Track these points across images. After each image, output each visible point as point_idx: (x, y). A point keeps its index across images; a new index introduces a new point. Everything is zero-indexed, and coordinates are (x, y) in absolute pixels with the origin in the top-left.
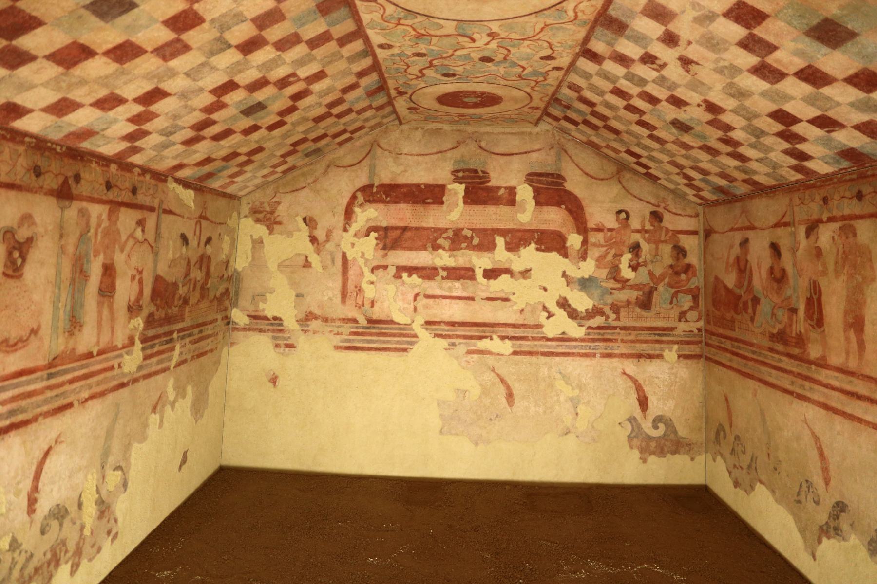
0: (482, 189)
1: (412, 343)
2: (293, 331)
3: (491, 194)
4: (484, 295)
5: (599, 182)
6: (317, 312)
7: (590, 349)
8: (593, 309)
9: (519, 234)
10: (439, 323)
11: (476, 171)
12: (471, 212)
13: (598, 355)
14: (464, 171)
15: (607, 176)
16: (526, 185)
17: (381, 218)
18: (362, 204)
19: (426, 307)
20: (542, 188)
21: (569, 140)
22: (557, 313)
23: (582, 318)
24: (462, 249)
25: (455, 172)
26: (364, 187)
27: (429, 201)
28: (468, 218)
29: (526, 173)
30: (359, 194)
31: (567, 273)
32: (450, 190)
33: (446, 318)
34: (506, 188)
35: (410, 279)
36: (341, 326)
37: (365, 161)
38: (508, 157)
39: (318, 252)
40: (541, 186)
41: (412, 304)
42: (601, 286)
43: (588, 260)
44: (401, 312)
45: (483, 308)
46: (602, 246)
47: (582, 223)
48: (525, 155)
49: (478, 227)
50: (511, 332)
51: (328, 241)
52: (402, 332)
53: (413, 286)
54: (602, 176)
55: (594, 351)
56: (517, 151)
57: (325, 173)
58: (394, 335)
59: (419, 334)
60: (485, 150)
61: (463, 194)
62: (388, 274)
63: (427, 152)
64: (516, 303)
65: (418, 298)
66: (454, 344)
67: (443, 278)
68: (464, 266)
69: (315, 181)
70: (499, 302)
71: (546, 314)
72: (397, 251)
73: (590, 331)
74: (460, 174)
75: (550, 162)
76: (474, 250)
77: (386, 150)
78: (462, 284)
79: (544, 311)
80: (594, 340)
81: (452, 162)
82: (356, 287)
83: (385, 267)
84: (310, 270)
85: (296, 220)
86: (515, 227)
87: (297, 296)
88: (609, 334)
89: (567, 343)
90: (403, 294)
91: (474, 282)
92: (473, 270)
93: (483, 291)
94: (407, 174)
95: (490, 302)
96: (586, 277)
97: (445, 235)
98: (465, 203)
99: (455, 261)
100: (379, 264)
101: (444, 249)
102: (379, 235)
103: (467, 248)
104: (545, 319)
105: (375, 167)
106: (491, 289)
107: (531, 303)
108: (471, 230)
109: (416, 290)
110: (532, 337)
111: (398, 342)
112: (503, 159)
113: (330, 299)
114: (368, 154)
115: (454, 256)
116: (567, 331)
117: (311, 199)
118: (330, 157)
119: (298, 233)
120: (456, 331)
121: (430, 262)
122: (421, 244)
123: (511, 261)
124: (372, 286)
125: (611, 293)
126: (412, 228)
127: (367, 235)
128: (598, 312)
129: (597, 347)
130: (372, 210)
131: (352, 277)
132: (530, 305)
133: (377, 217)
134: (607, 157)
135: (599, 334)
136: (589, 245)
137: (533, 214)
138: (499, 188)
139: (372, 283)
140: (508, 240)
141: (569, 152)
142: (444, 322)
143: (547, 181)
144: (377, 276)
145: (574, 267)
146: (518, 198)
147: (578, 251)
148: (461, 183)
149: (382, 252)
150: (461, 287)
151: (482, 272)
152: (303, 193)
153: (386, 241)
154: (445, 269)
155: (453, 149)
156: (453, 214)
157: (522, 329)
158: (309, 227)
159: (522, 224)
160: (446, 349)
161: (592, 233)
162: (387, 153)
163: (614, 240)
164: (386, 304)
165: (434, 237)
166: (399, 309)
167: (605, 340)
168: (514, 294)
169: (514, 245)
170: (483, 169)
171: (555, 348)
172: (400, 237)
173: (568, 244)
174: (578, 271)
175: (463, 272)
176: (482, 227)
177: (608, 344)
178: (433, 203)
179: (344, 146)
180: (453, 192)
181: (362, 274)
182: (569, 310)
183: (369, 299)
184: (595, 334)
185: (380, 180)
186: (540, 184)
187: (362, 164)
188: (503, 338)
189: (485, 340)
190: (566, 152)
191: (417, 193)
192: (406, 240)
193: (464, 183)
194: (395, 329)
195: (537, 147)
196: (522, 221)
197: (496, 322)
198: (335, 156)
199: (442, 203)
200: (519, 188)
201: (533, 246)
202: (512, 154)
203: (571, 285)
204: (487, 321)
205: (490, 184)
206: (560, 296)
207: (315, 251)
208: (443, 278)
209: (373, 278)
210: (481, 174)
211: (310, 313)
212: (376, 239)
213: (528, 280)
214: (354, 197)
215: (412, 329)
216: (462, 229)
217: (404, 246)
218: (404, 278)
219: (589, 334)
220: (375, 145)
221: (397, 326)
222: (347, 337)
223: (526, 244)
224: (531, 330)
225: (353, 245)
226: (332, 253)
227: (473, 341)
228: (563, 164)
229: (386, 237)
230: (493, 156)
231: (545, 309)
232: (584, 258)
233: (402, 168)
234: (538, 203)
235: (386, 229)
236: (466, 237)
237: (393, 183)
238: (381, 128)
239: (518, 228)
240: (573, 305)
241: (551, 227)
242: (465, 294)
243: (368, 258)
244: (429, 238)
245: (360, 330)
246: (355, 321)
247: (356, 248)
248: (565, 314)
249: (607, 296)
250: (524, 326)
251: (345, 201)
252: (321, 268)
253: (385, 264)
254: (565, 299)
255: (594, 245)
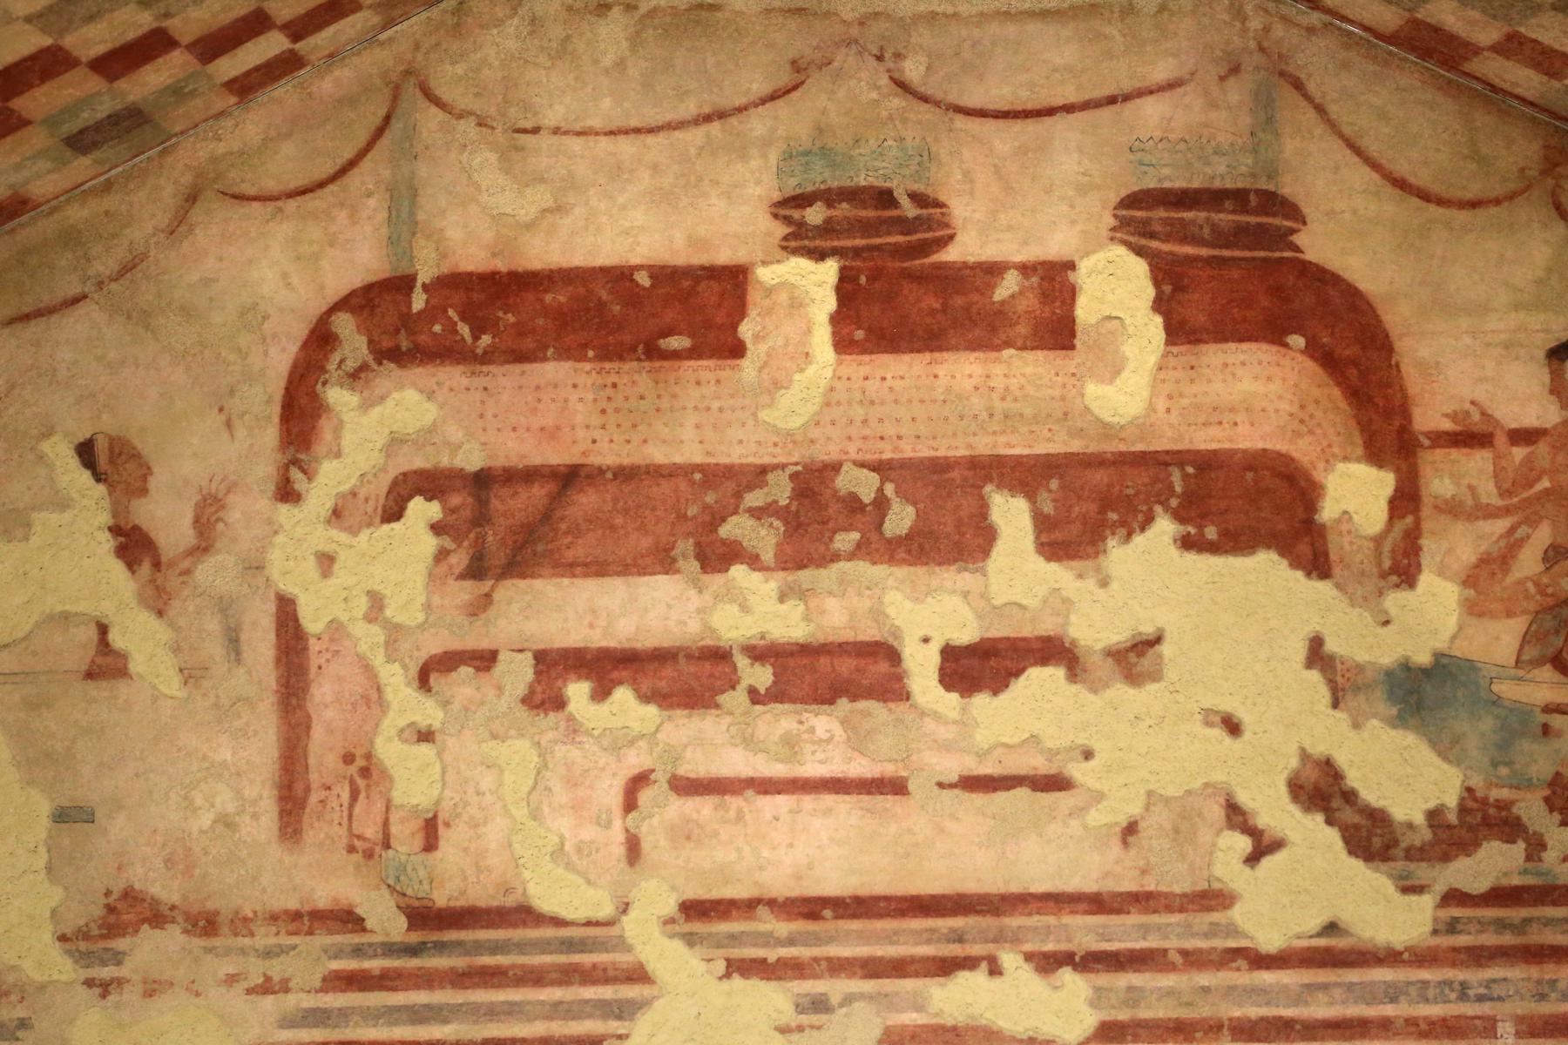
0: (919, 278)
1: (624, 1011)
2: (42, 987)
3: (959, 301)
4: (953, 766)
5: (1463, 216)
6: (165, 889)
7: (1463, 996)
8: (1463, 810)
9: (1100, 477)
10: (749, 906)
11: (885, 198)
12: (873, 386)
13: (1506, 1029)
14: (829, 197)
15: (1498, 190)
16: (1120, 251)
17: (454, 433)
18: (364, 367)
19: (685, 834)
20: (1196, 259)
21: (1311, 30)
22: (1292, 835)
23: (1417, 854)
24: (836, 557)
25: (789, 205)
26: (369, 288)
27: (676, 342)
28: (859, 412)
29: (1114, 198)
30: (345, 325)
31: (1331, 646)
32: (770, 291)
33: (779, 884)
34: (1026, 269)
35: (603, 709)
36: (282, 951)
37: (367, 164)
38: (1031, 127)
39: (158, 602)
40: (1189, 250)
41: (618, 824)
42: (1496, 701)
43: (1426, 579)
44: (569, 866)
45: (950, 825)
46: (1490, 513)
47: (1388, 414)
48: (1106, 113)
49: (908, 453)
50: (1085, 932)
51: (203, 546)
52: (576, 958)
53: (620, 742)
54: (1474, 190)
55: (1486, 1009)
56: (1070, 95)
57: (179, 225)
58: (536, 978)
59: (653, 966)
60: (925, 99)
61: (831, 304)
62: (500, 689)
63: (654, 116)
64: (1099, 797)
65: (645, 796)
66: (819, 1005)
67: (755, 696)
68: (849, 636)
69: (126, 269)
70: (1022, 793)
71: (1244, 844)
72: (538, 584)
73: (1457, 912)
74: (815, 215)
75: (1223, 139)
76: (892, 560)
77: (460, 116)
78: (844, 722)
79: (1231, 825)
80: (1478, 956)
81: (773, 157)
82: (348, 759)
83: (485, 660)
84: (123, 689)
85: (41, 458)
86: (1076, 446)
87: (62, 816)
88: (1549, 922)
89: (1353, 976)
90: (572, 783)
91: (899, 708)
92: (892, 655)
93: (946, 747)
94: (566, 222)
95: (979, 799)
96: (1423, 658)
97: (754, 499)
98: (843, 345)
99: (807, 618)
100: (456, 645)
101: (754, 562)
102: (449, 511)
103: (861, 551)
104: (1238, 866)
105: (414, 194)
106: (983, 737)
107: (1171, 791)
108: (879, 467)
109: (636, 761)
110: (1184, 953)
111: (556, 1010)
112: (1004, 137)
113: (226, 822)
114: (379, 133)
115: (803, 594)
116: (1346, 916)
117: (112, 355)
118: (194, 153)
119: (54, 518)
120: (830, 940)
121: (694, 627)
122: (646, 543)
123: (1067, 601)
124: (425, 749)
125: (1546, 730)
126: (601, 471)
127: (393, 513)
128: (1487, 822)
129: (1497, 990)
130: (411, 395)
131: (329, 714)
132: (1167, 801)
133: (433, 429)
134: (1494, 95)
135: (1502, 925)
136: (1426, 511)
137: (1156, 382)
138: (994, 270)
139: (425, 736)
140: (1048, 508)
141: (1311, 87)
142: (772, 903)
143: (1215, 228)
144: (445, 704)
145: (1361, 618)
146: (1085, 311)
147: (1378, 540)
148: (819, 255)
149: (467, 590)
150: (838, 731)
151: (936, 659)
152: (75, 324)
153: (480, 542)
154: (760, 653)
155: (773, 97)
156: (786, 399)
157: (1133, 919)
158: (112, 487)
159: (1107, 430)
160: (784, 1030)
161: (1439, 453)
162: (467, 127)
163: (1545, 483)
164: (495, 831)
165: (706, 507)
166: (559, 853)
167: (1535, 954)
168: (1088, 755)
169: (1075, 529)
170: (919, 187)
171: (1298, 1001)
172: (546, 517)
173: (1328, 512)
174: (1383, 631)
175: (846, 666)
176: (924, 452)
177: (1549, 971)
178: (694, 353)
179: (262, 97)
180: (783, 297)
181: (373, 698)
182: (1349, 815)
183: (415, 810)
184: (1483, 925)
185: (444, 256)
186: (1184, 240)
187: (355, 179)
188: (1048, 963)
189: (963, 977)
190: (1298, 85)
191: (616, 309)
192: (576, 531)
193: (835, 252)
194: (544, 946)
195: (1162, 71)
196: (1106, 416)
197: (1015, 888)
198: (221, 148)
199: (737, 350)
200: (1084, 266)
201: (1165, 528)
202: (1050, 112)
203: (1350, 701)
204: (970, 886)
205: (951, 254)
206: (1304, 755)
207: (143, 601)
208: (755, 696)
209: (428, 712)
210: (909, 210)
211: (129, 895)
212: (437, 528)
213: (1152, 687)
214: (321, 339)
215: (622, 944)
216: (836, 467)
217: (569, 555)
218: (572, 707)
219: (1452, 927)
220: (411, 91)
221: (549, 932)
222: (310, 1001)
223: (1134, 520)
224: (1175, 918)
225: (326, 562)
226: (225, 606)
227: (908, 985)
228: (1290, 146)
229: (481, 518)
230: (961, 122)
231: (1236, 816)
232: (1404, 571)
233: (537, 199)
234: (1179, 332)
235: (482, 481)
236: (853, 504)
237: (501, 265)
238: (435, 12)
239: (1093, 448)
240: (1370, 795)
241: (1247, 438)
242: (860, 768)
243: (398, 619)
244: (682, 517)
245: (375, 965)
246: (348, 919)
247: (342, 576)
248: (1333, 836)
249: (1526, 745)
250: (1142, 900)
251: (280, 359)
252: (176, 681)
253: (485, 644)
254: (1328, 767)
255: (1452, 509)
